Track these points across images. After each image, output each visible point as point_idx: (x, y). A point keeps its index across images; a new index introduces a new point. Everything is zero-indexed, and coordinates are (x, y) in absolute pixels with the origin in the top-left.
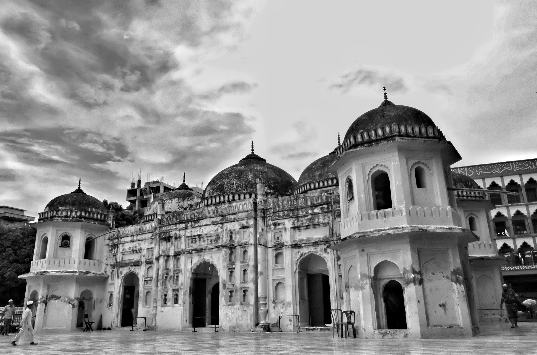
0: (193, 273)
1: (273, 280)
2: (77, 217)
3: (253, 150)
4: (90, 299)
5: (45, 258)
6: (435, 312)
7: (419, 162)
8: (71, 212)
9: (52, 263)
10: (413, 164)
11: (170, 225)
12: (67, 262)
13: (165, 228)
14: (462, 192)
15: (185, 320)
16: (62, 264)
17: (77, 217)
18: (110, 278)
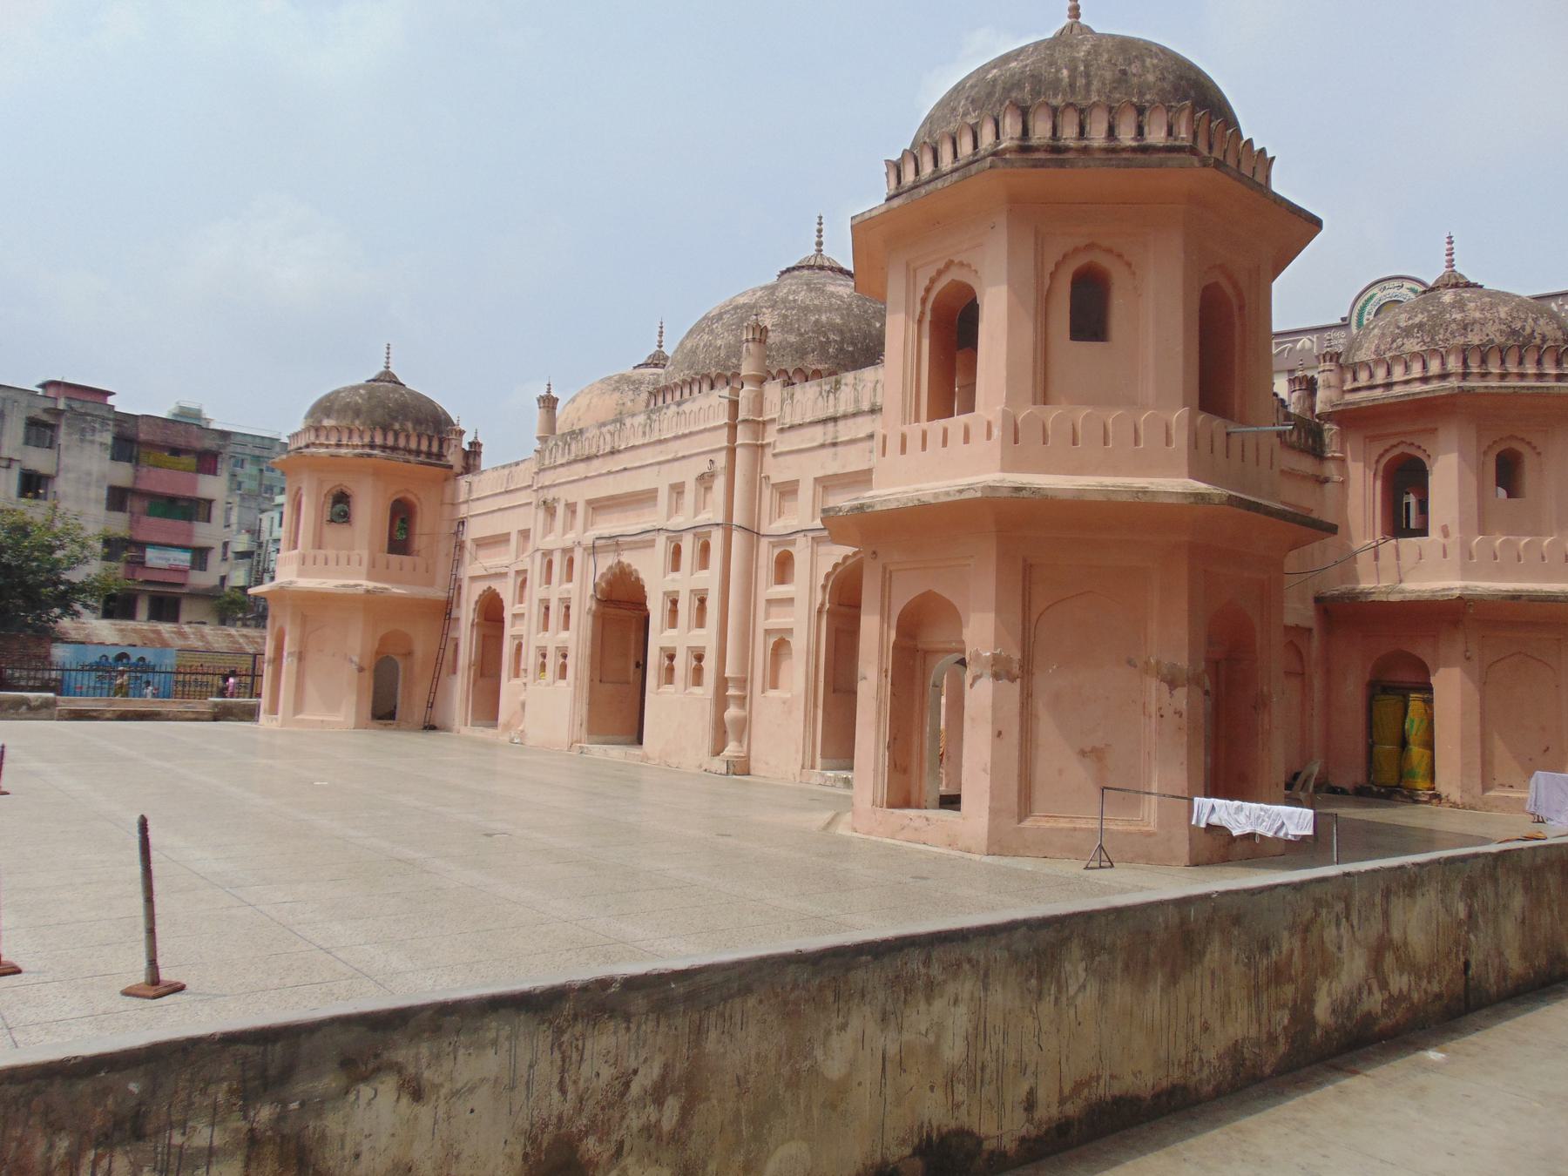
1: (768, 632)
2: (363, 446)
3: (820, 244)
4: (409, 654)
5: (295, 547)
6: (1060, 772)
7: (1090, 247)
8: (351, 431)
9: (309, 561)
10: (1065, 256)
11: (555, 467)
12: (343, 561)
13: (547, 478)
14: (1484, 361)
15: (578, 722)
17: (363, 446)
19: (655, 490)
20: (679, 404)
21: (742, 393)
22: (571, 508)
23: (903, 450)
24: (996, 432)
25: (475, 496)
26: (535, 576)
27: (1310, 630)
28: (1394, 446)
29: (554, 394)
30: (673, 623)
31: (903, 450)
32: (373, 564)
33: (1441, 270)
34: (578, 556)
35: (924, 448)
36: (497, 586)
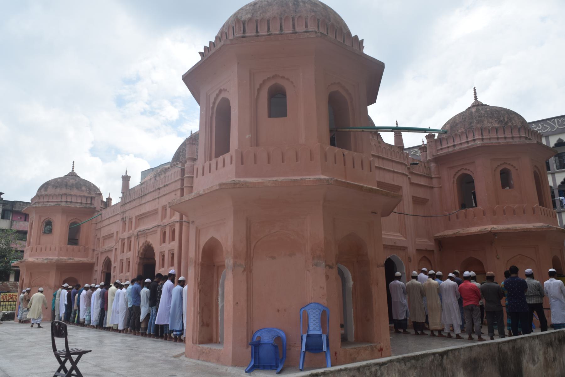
0: (140, 258)
9: (34, 250)
16: (43, 250)
18: (96, 264)
19: (157, 209)
20: (165, 173)
21: (186, 165)
22: (130, 219)
23: (203, 174)
24: (234, 162)
25: (104, 219)
26: (119, 251)
27: (433, 251)
28: (459, 171)
29: (128, 175)
30: (163, 266)
31: (203, 174)
32: (61, 249)
33: (473, 101)
34: (133, 239)
35: (210, 172)
36: (109, 255)
